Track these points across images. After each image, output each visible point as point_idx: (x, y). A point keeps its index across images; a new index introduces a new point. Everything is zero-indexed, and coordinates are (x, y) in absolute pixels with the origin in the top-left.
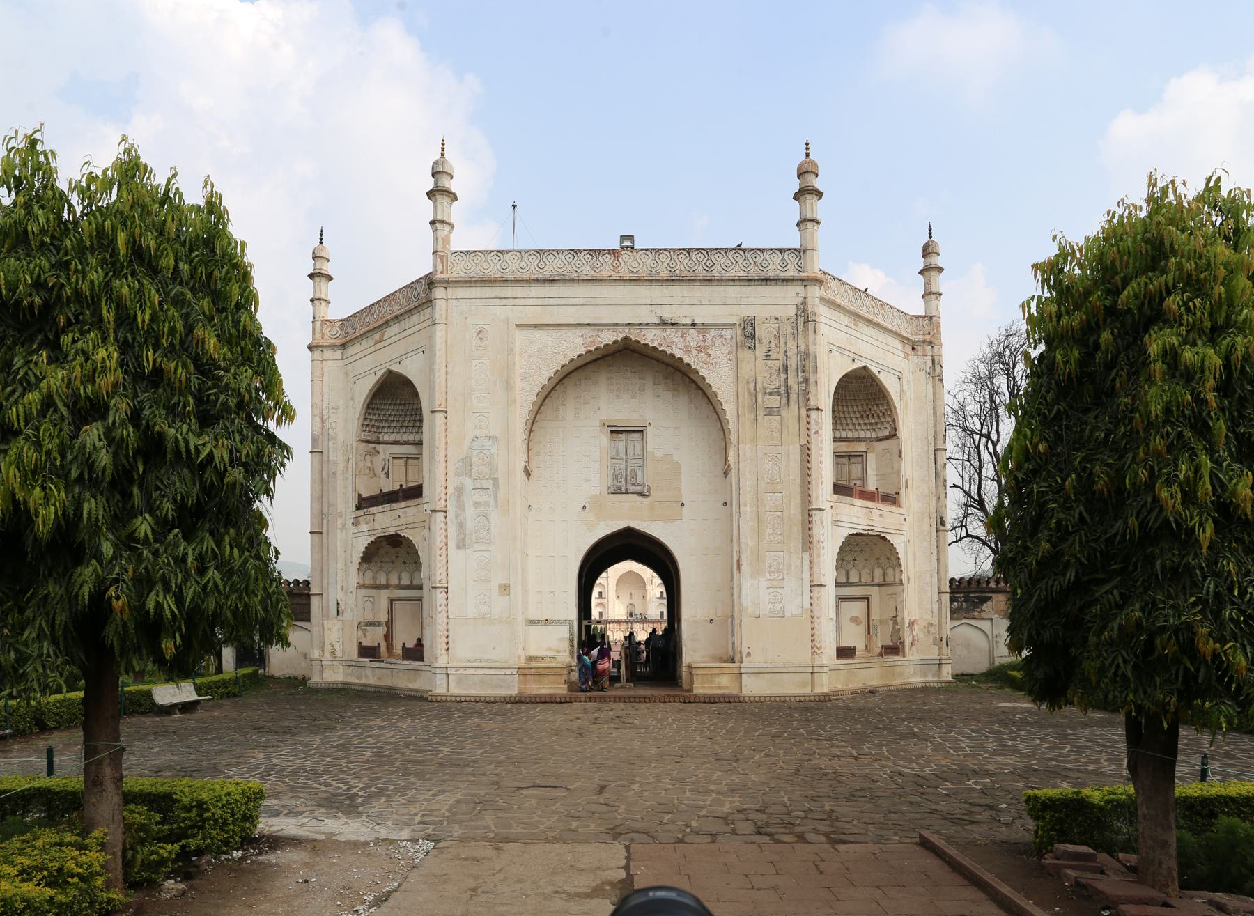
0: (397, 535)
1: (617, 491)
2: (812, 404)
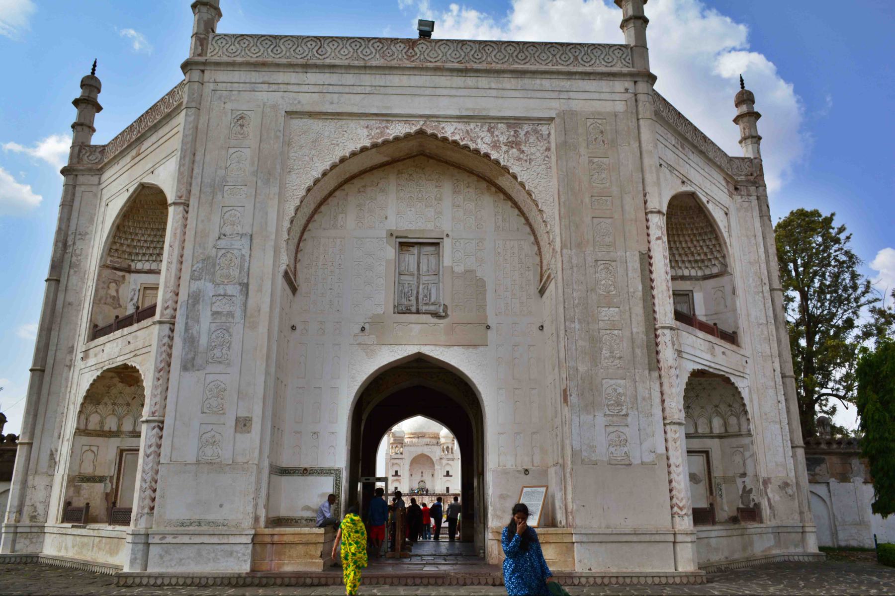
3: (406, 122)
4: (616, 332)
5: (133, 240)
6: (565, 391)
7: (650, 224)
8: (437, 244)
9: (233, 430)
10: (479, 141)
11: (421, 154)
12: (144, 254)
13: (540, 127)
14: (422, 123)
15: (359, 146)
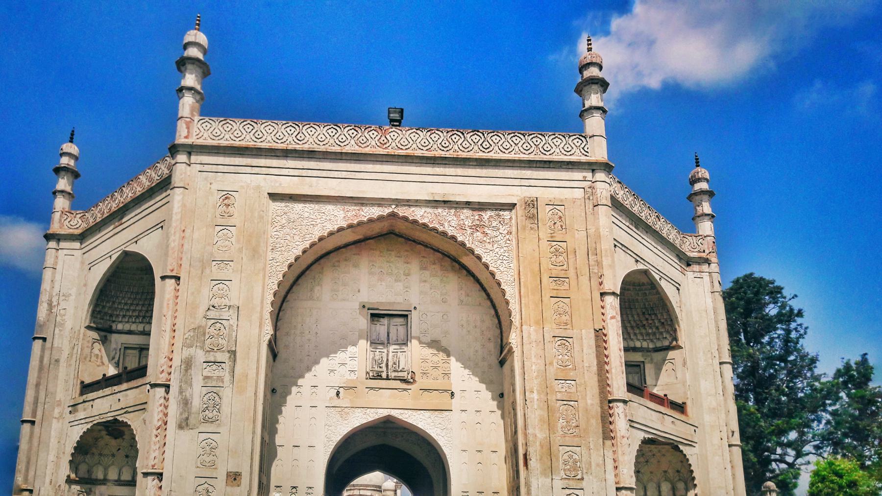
0: (116, 419)
5: (114, 302)
8: (407, 316)
9: (224, 483)
10: (446, 224)
11: (391, 233)
12: (124, 316)
15: (336, 227)
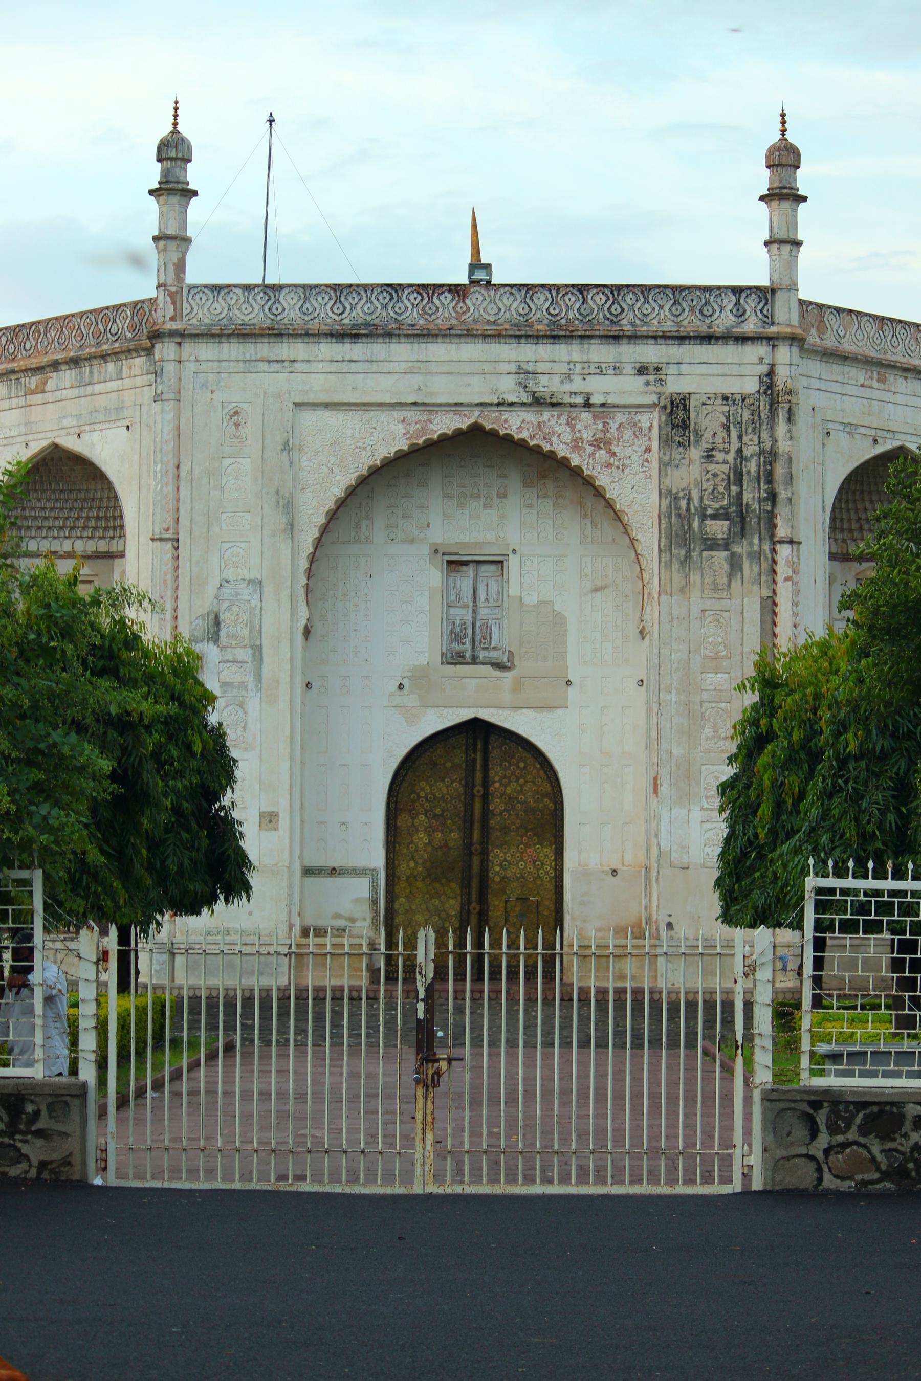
1: (456, 659)
2: (782, 532)
3: (456, 413)
4: (723, 705)
6: (655, 779)
7: (778, 558)
10: (555, 439)
13: (639, 417)
14: (477, 413)
